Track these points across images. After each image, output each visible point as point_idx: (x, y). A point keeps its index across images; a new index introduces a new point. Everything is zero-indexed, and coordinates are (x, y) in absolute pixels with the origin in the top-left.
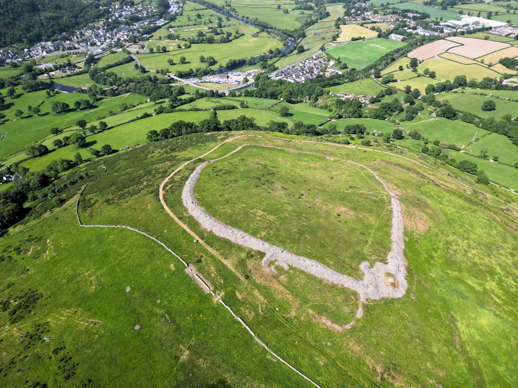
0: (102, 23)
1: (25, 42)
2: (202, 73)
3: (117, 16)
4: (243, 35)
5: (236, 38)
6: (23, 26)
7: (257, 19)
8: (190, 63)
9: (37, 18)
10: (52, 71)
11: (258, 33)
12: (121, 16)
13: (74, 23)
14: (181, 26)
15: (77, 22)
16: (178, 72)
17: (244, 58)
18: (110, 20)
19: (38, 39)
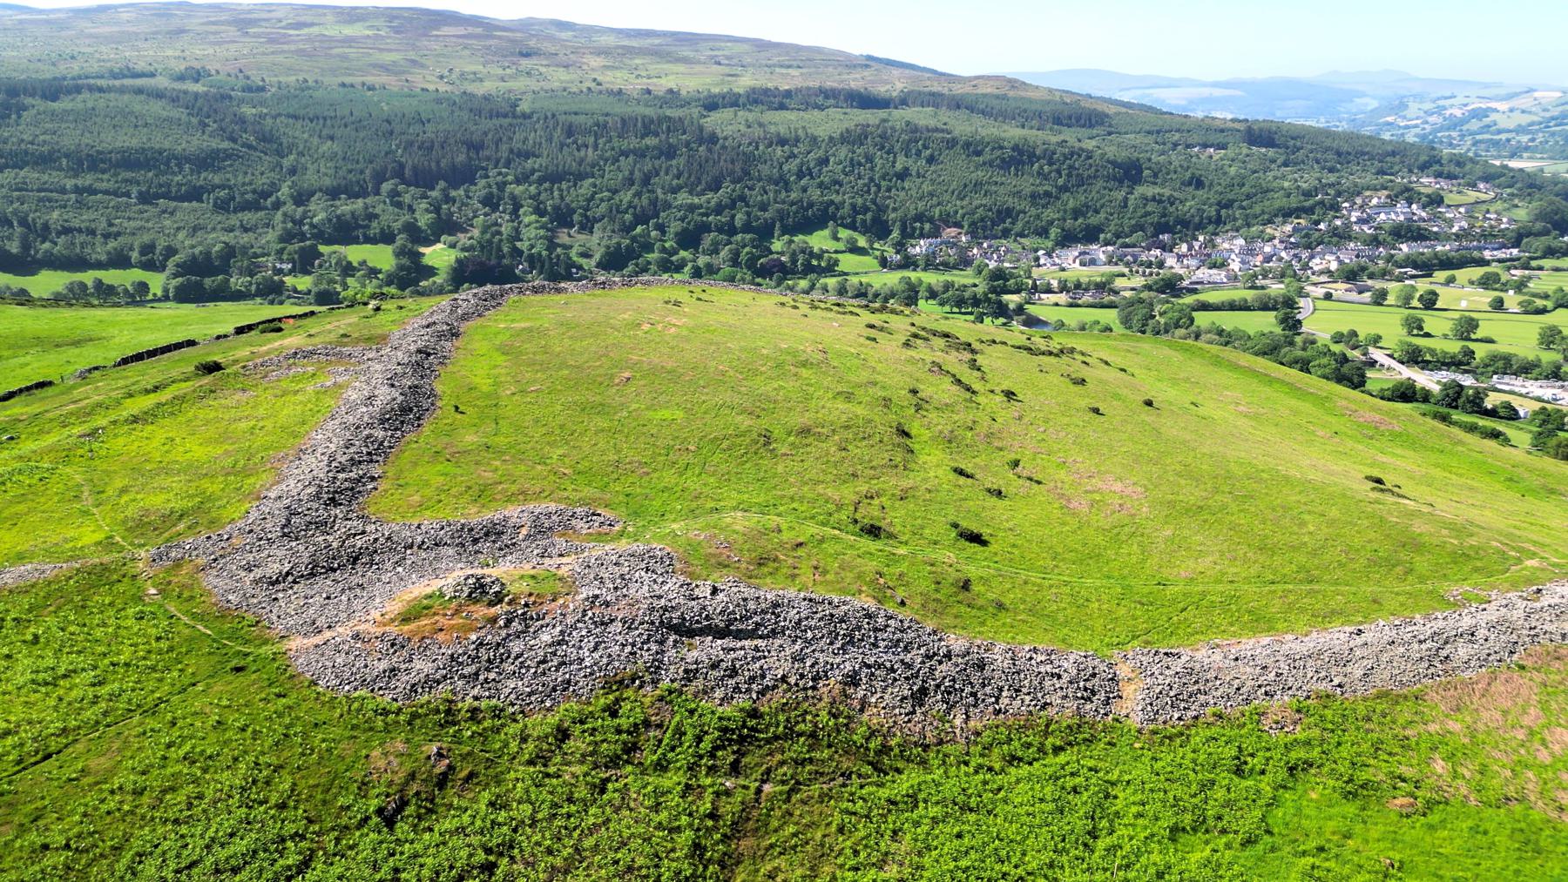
0: (1288, 228)
1: (1052, 236)
2: (1500, 364)
3: (1353, 219)
6: (1071, 204)
8: (1491, 341)
9: (1119, 195)
10: (1049, 291)
12: (1361, 221)
13: (1209, 219)
15: (1219, 216)
16: (1410, 345)
18: (1322, 226)
19: (1091, 235)
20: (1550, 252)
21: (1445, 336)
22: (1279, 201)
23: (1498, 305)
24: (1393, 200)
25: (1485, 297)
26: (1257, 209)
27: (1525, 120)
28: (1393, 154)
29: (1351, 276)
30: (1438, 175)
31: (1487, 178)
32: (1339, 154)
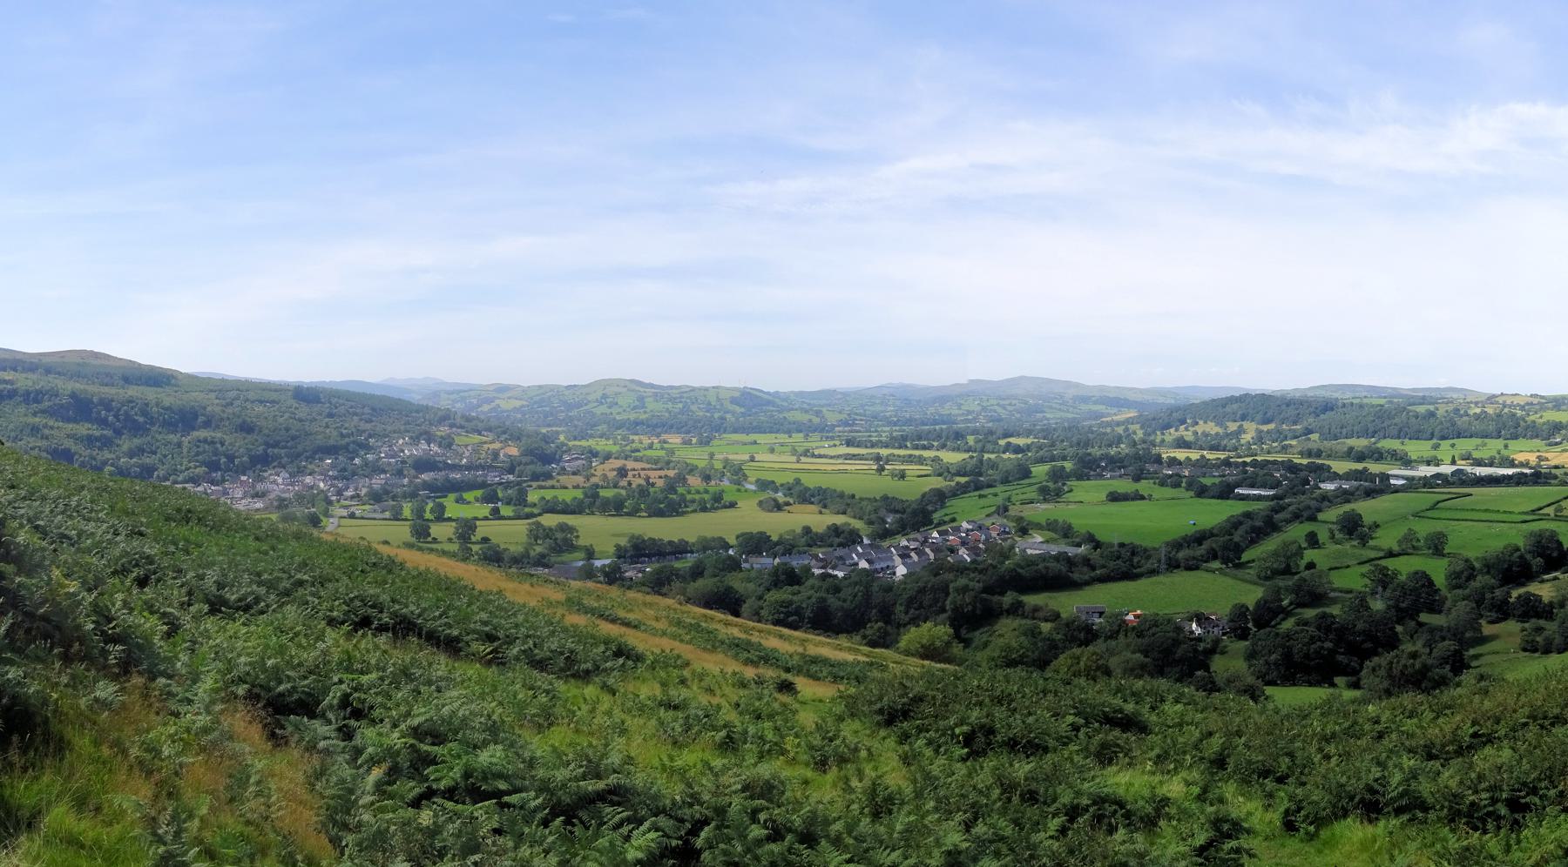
4: (732, 505)
5: (704, 509)
7: (798, 481)
11: (788, 504)
14: (553, 487)
17: (692, 539)
18: (357, 461)
20: (535, 477)
21: (450, 540)
22: (320, 441)
23: (495, 513)
24: (415, 440)
25: (485, 510)
26: (300, 448)
27: (518, 403)
28: (417, 412)
29: (376, 497)
30: (451, 426)
31: (490, 430)
32: (373, 409)
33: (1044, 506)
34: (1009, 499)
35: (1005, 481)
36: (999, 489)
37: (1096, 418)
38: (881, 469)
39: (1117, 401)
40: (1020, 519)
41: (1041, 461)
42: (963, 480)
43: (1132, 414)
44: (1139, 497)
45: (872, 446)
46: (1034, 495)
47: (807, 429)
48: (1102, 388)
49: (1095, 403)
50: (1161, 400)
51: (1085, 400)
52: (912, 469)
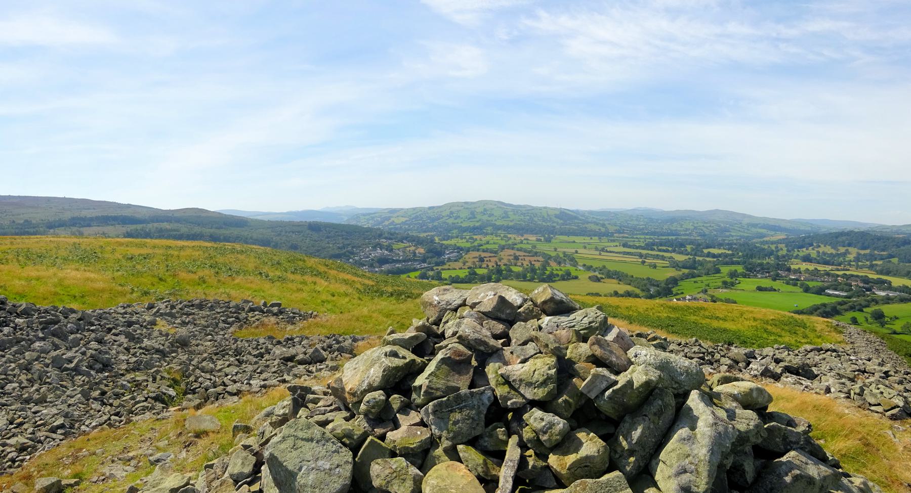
33: (725, 290)
34: (708, 285)
35: (707, 274)
36: (704, 278)
37: (761, 237)
38: (643, 262)
39: (775, 227)
40: (712, 297)
41: (727, 264)
42: (686, 271)
43: (781, 236)
44: (772, 290)
45: (637, 248)
46: (720, 284)
47: (600, 235)
48: (765, 219)
49: (762, 227)
50: (802, 228)
51: (755, 226)
52: (659, 262)
